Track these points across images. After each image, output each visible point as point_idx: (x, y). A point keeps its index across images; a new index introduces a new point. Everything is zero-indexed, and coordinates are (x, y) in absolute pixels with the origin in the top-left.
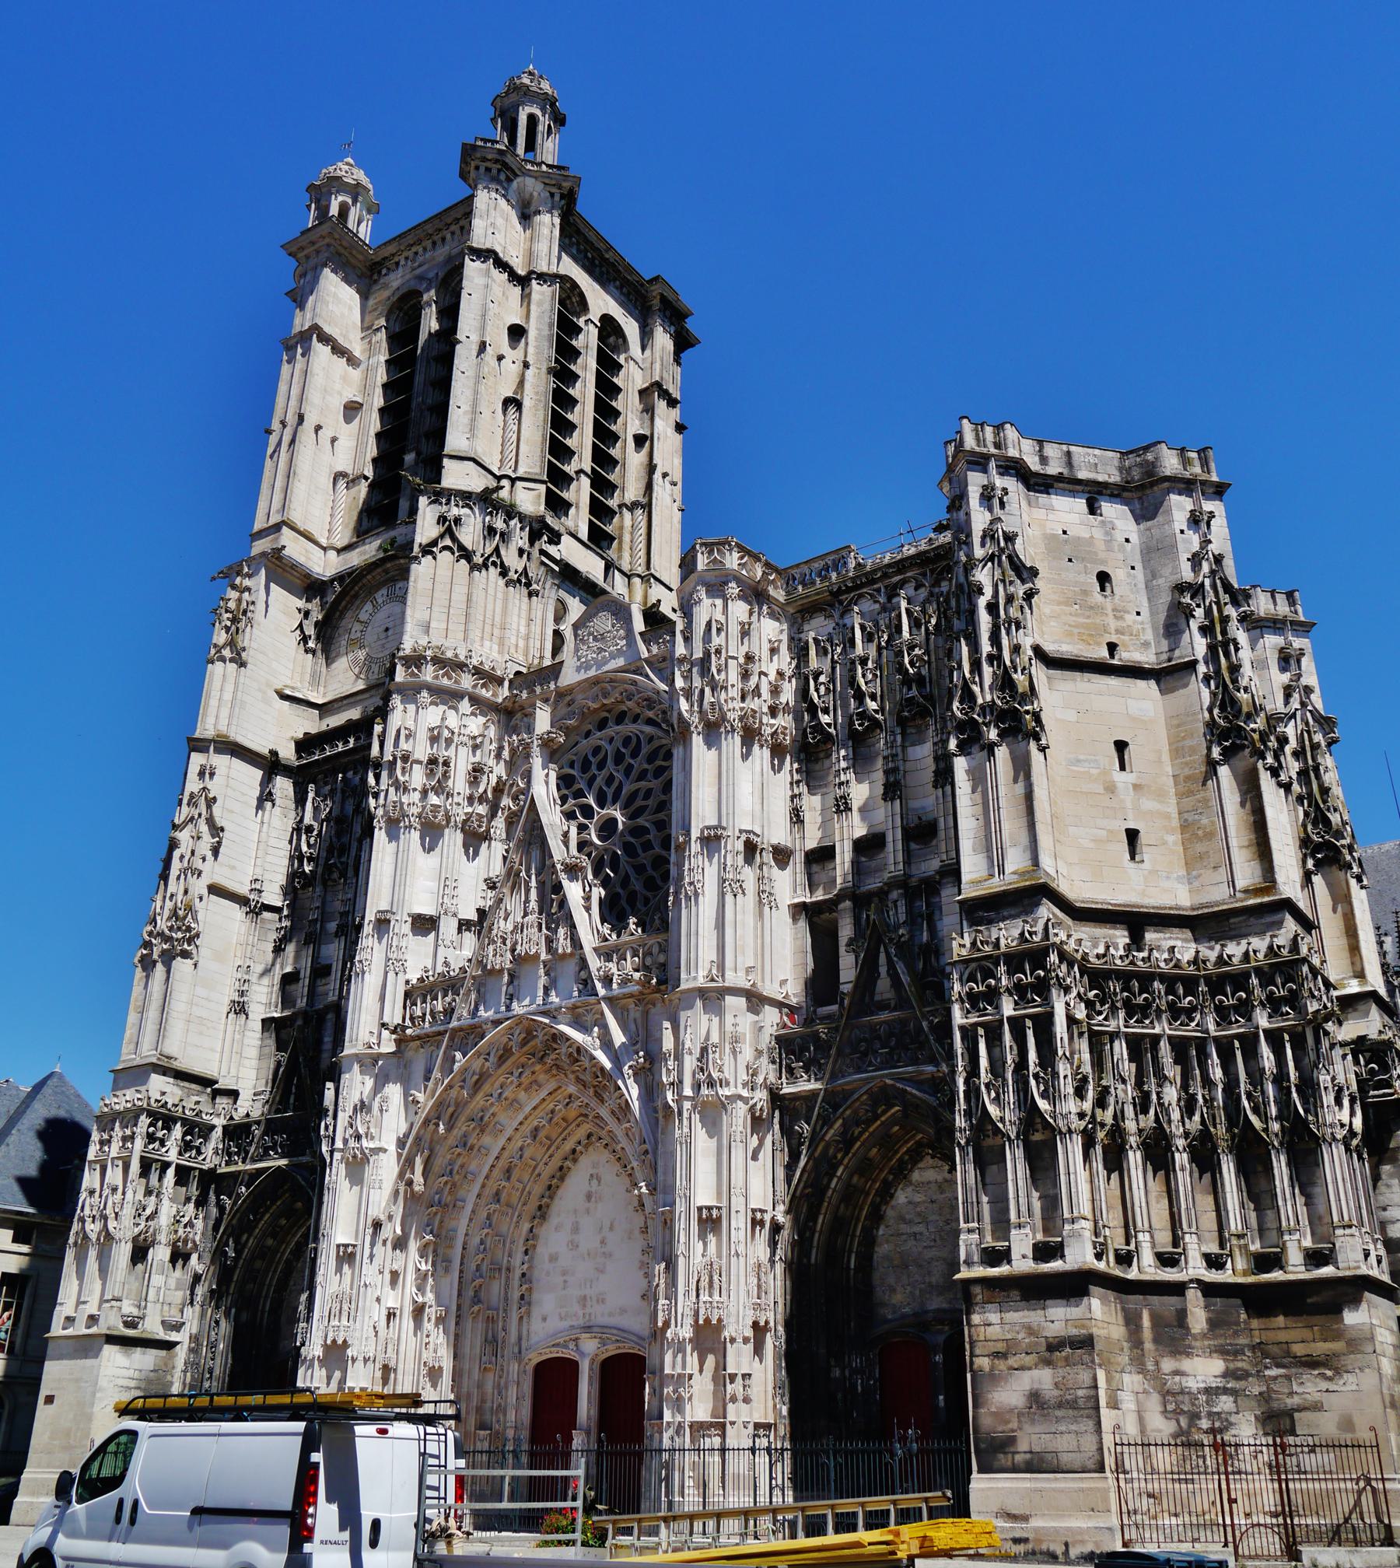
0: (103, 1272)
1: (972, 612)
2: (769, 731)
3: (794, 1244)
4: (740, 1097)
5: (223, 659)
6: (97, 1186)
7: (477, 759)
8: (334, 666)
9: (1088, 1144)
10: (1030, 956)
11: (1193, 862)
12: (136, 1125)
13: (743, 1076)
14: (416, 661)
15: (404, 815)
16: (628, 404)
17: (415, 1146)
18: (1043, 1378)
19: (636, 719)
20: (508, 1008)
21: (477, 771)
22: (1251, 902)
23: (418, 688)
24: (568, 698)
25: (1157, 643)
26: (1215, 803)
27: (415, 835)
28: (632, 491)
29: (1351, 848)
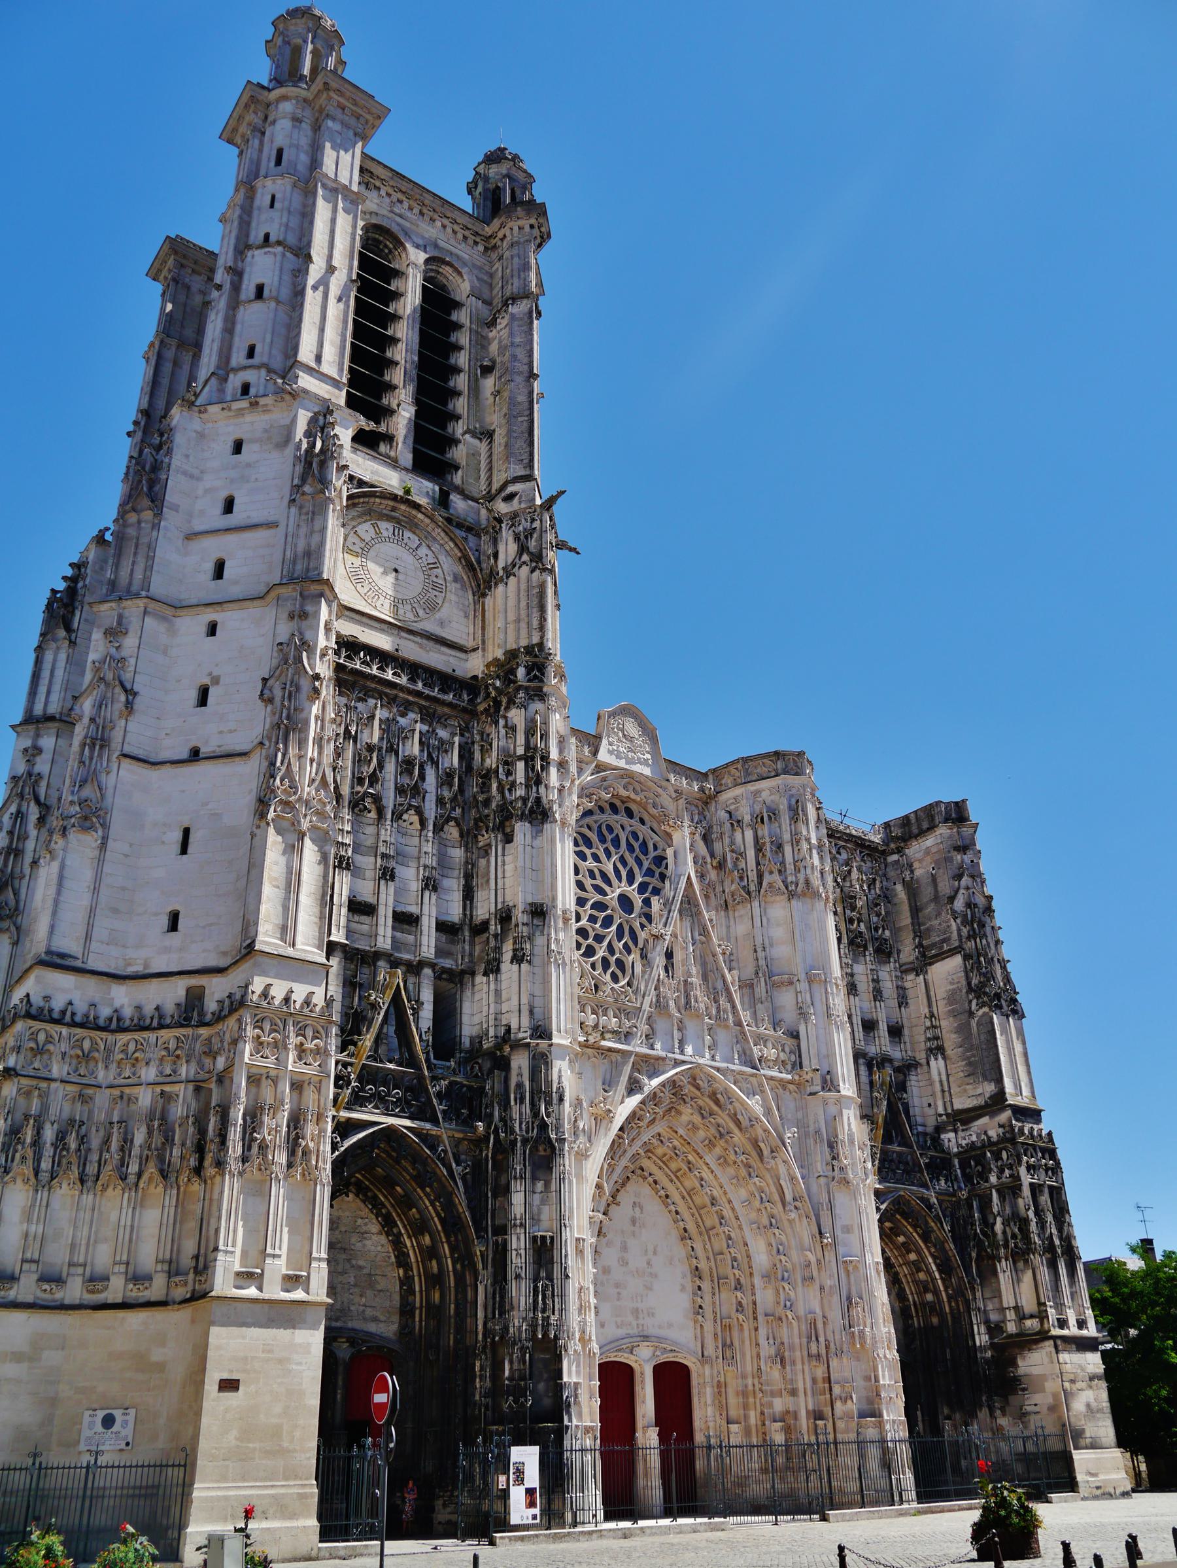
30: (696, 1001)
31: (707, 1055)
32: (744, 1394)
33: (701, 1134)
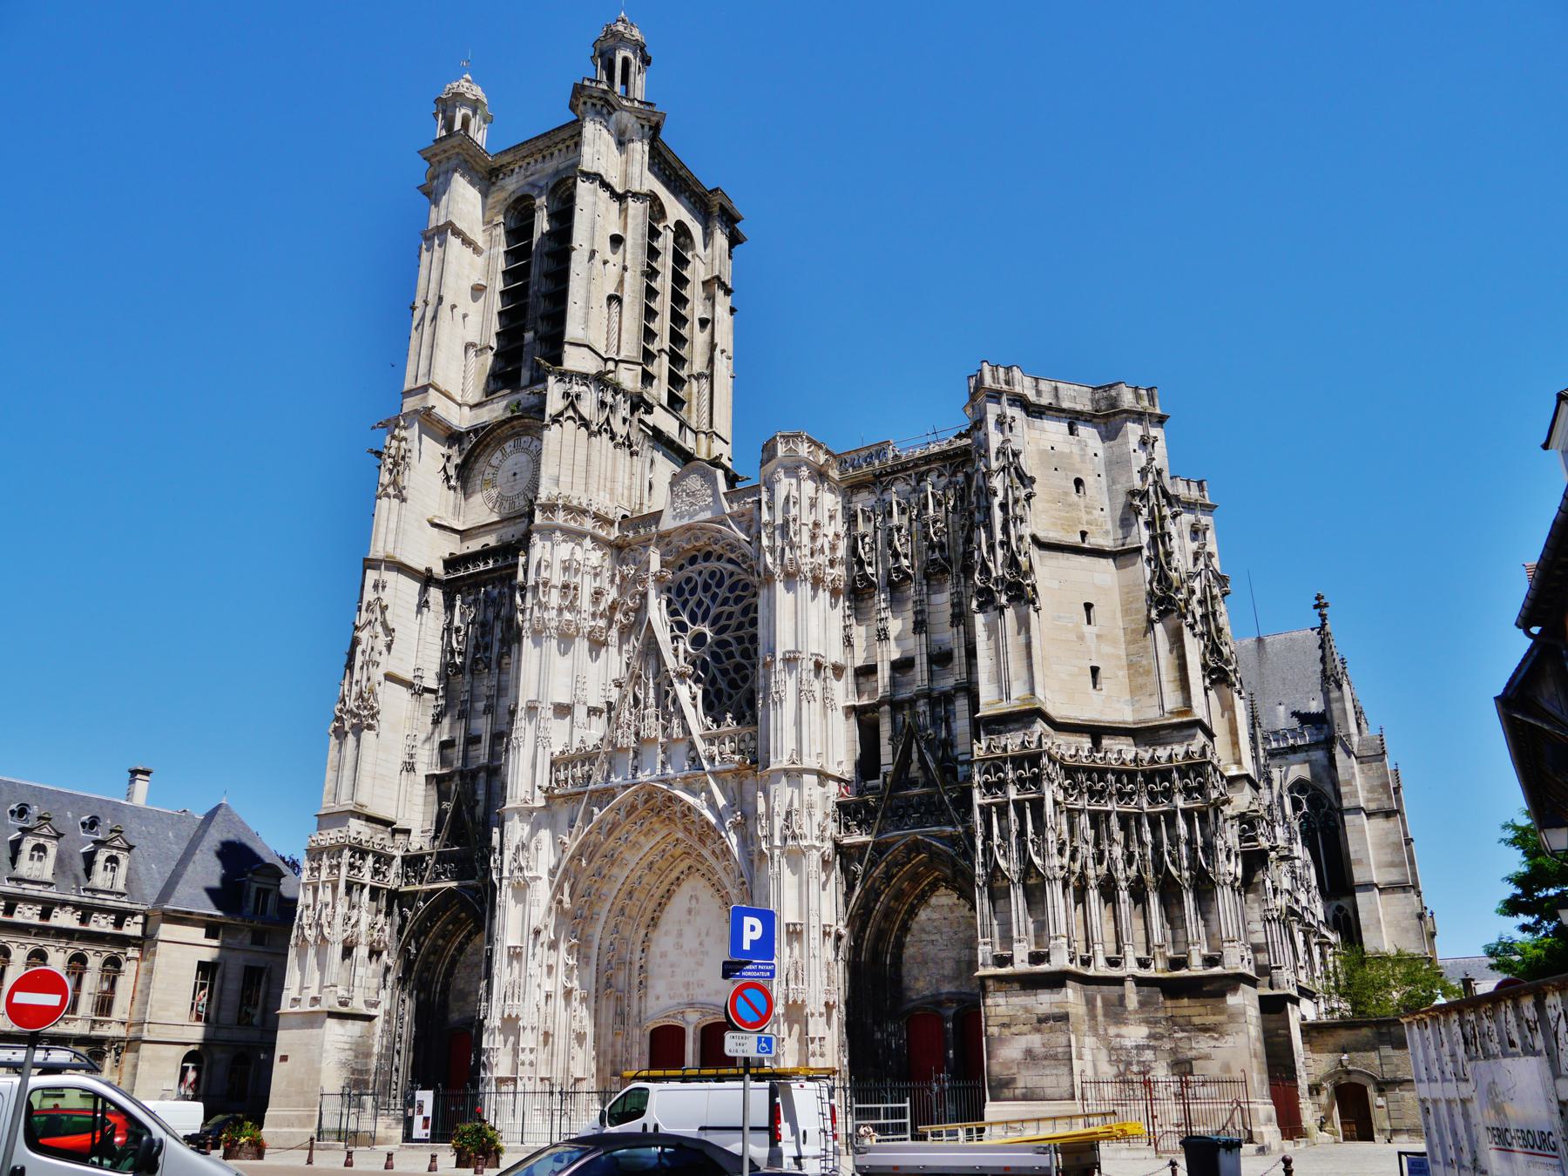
0: (322, 966)
1: (989, 508)
2: (830, 578)
3: (851, 948)
4: (815, 847)
5: (388, 496)
6: (311, 901)
7: (597, 584)
8: (471, 500)
9: (1065, 885)
10: (1030, 759)
11: (1135, 690)
12: (340, 856)
13: (816, 832)
14: (550, 508)
15: (546, 628)
16: (694, 292)
17: (566, 875)
18: (1035, 1041)
19: (719, 558)
20: (634, 776)
21: (598, 594)
22: (1176, 720)
23: (553, 530)
24: (667, 540)
25: (1114, 534)
26: (1152, 649)
27: (554, 643)
28: (698, 364)
29: (1235, 671)
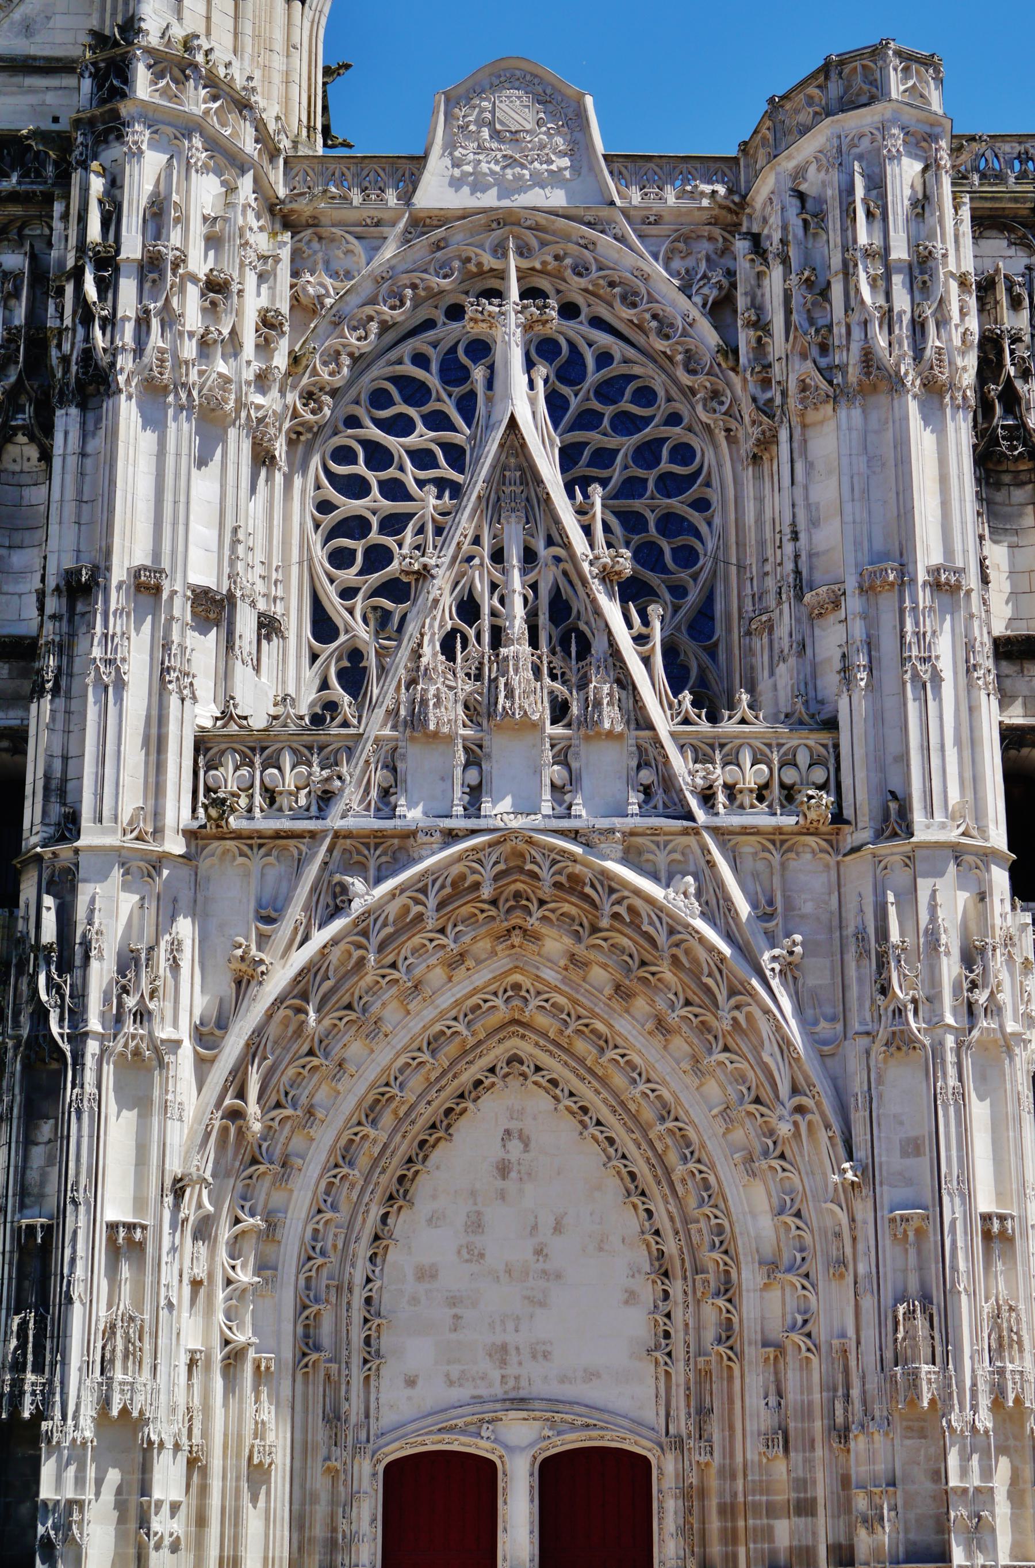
23: (188, 128)
30: (510, 695)
31: (546, 808)
32: (727, 1510)
33: (598, 975)
